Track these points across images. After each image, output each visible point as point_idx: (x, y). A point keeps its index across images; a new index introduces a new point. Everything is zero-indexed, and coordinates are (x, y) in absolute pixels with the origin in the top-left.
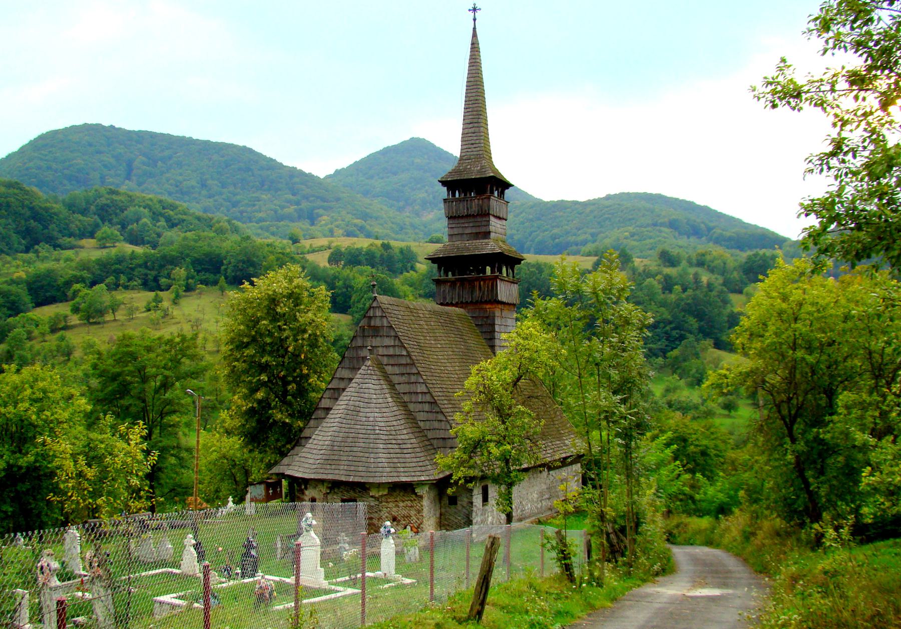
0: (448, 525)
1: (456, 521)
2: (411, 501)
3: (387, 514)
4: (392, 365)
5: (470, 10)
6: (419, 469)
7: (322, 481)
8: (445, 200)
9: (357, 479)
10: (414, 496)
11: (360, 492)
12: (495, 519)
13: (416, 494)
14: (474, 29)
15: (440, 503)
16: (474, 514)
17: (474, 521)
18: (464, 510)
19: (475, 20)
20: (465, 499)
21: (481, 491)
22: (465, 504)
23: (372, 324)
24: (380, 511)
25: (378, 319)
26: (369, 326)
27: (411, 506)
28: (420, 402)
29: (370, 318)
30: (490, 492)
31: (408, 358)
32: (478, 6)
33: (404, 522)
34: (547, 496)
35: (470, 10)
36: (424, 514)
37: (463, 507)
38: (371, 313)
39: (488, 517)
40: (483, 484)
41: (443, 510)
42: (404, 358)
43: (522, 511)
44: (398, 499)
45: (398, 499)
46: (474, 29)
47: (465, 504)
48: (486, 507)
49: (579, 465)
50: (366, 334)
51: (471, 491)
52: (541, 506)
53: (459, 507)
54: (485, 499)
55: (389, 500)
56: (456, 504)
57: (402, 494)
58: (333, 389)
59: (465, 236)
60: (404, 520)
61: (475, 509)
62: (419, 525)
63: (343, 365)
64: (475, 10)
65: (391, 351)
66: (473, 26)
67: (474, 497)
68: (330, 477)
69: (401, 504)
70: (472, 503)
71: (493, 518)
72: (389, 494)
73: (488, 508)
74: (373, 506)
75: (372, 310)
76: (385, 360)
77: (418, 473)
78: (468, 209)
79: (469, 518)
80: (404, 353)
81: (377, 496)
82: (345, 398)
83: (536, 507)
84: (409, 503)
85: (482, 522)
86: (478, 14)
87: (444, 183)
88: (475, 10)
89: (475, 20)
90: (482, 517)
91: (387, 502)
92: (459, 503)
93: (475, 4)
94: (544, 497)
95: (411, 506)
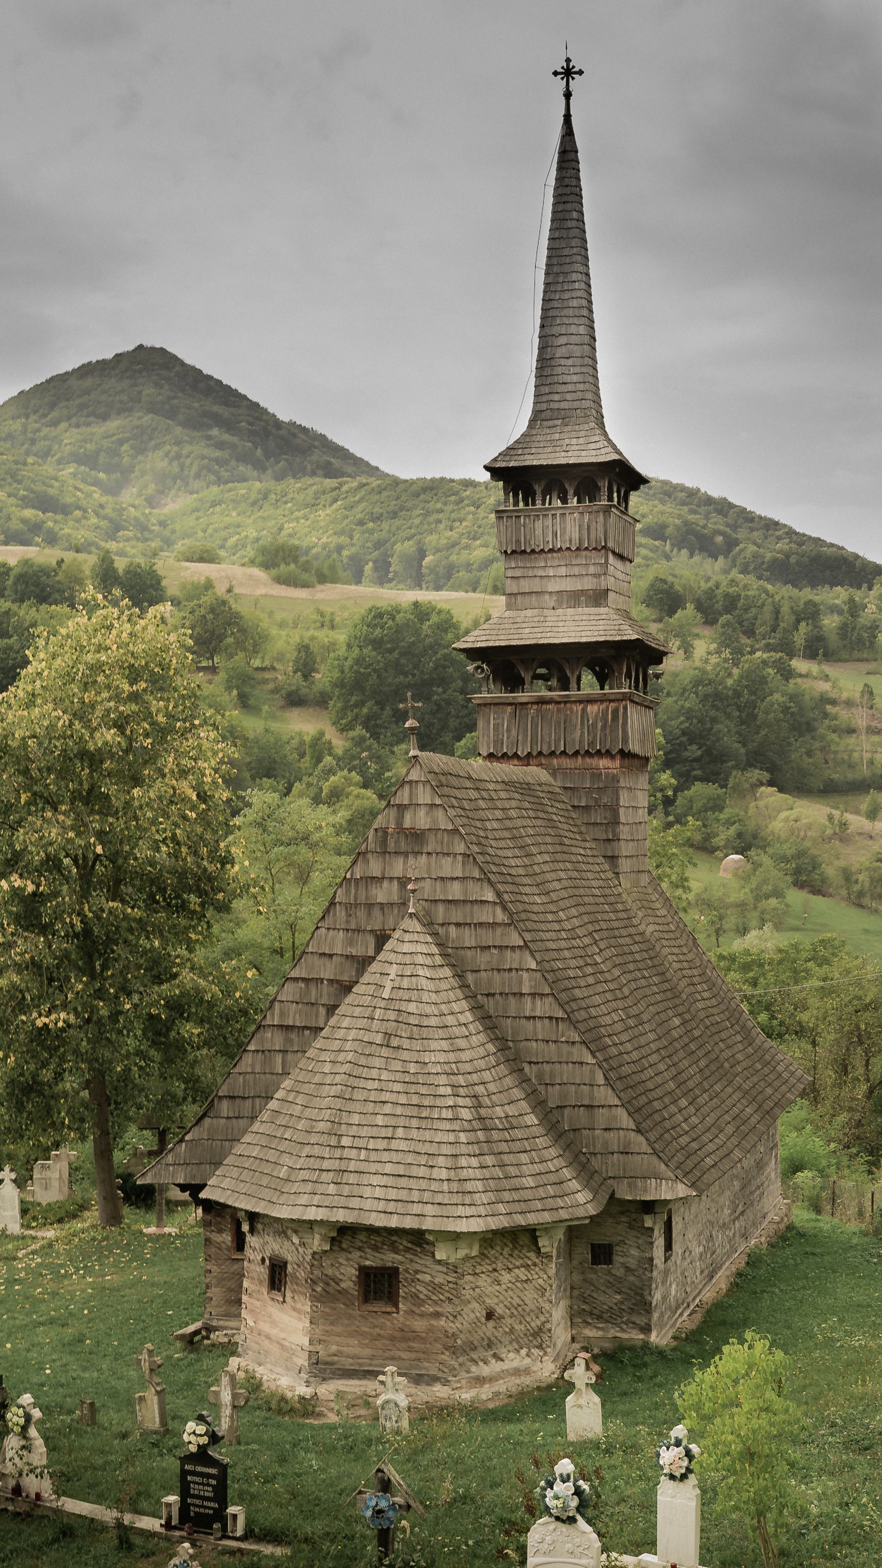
2: (527, 1267)
4: (458, 925)
5: (556, 73)
7: (311, 1225)
8: (500, 514)
9: (409, 1223)
10: (532, 1255)
11: (408, 1249)
14: (567, 117)
19: (568, 95)
20: (634, 1252)
22: (632, 1263)
23: (407, 823)
25: (422, 812)
26: (400, 829)
27: (526, 1281)
28: (528, 1018)
29: (402, 808)
31: (499, 910)
32: (576, 64)
35: (556, 73)
37: (628, 1269)
38: (403, 797)
39: (670, 1285)
42: (490, 908)
44: (499, 1266)
45: (499, 1266)
46: (567, 117)
50: (391, 846)
54: (668, 1247)
56: (609, 1261)
57: (506, 1251)
58: (303, 979)
59: (547, 597)
63: (329, 922)
64: (568, 72)
65: (455, 891)
66: (563, 112)
68: (341, 1216)
69: (506, 1277)
72: (483, 1255)
74: (440, 1286)
75: (407, 788)
76: (440, 913)
78: (555, 534)
80: (490, 896)
82: (357, 1011)
84: (522, 1273)
86: (575, 84)
87: (487, 468)
88: (568, 72)
89: (568, 95)
92: (618, 1259)
93: (568, 60)
95: (526, 1281)
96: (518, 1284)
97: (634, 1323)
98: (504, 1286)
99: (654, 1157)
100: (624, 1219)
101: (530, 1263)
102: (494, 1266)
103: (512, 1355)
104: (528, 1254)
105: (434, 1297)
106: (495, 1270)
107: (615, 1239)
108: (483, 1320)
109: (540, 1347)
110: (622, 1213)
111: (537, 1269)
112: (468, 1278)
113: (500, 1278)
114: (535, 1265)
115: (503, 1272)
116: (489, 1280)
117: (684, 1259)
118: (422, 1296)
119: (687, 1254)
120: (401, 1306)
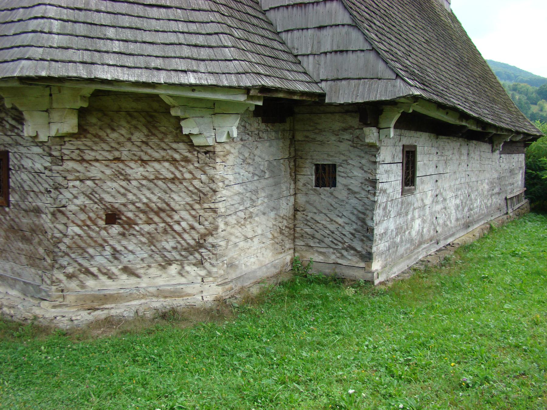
0: (313, 237)
1: (332, 227)
2: (173, 161)
3: (81, 200)
6: (186, 51)
12: (426, 226)
13: (188, 140)
15: (295, 181)
16: (379, 213)
17: (378, 230)
18: (353, 201)
20: (358, 173)
21: (399, 158)
22: (355, 185)
24: (57, 188)
27: (173, 180)
30: (419, 164)
33: (147, 228)
34: (497, 190)
36: (221, 208)
39: (413, 219)
40: (406, 141)
41: (302, 199)
43: (470, 210)
45: (125, 154)
47: (355, 185)
48: (411, 198)
49: (522, 157)
51: (374, 149)
52: (491, 204)
53: (340, 191)
55: (89, 155)
57: (138, 137)
60: (149, 222)
61: (381, 199)
62: (203, 236)
67: (381, 169)
70: (374, 183)
71: (424, 221)
73: (415, 199)
77: (182, 65)
79: (363, 221)
81: (43, 137)
83: (486, 204)
85: (399, 230)
90: (400, 221)
91: (82, 160)
92: (339, 180)
94: (495, 191)
95: (173, 180)
96: (160, 183)
97: (355, 250)
98: (134, 183)
99: (372, 56)
100: (347, 136)
101: (177, 156)
102: (117, 154)
103: (154, 271)
104: (174, 146)
105: (35, 189)
106: (118, 159)
107: (337, 160)
108: (102, 223)
109: (200, 264)
110: (345, 130)
111: (191, 167)
112: (70, 165)
113: (129, 171)
114: (187, 160)
115: (132, 164)
116: (108, 172)
117: (435, 201)
118: (27, 188)
119: (440, 199)
120: (11, 199)
